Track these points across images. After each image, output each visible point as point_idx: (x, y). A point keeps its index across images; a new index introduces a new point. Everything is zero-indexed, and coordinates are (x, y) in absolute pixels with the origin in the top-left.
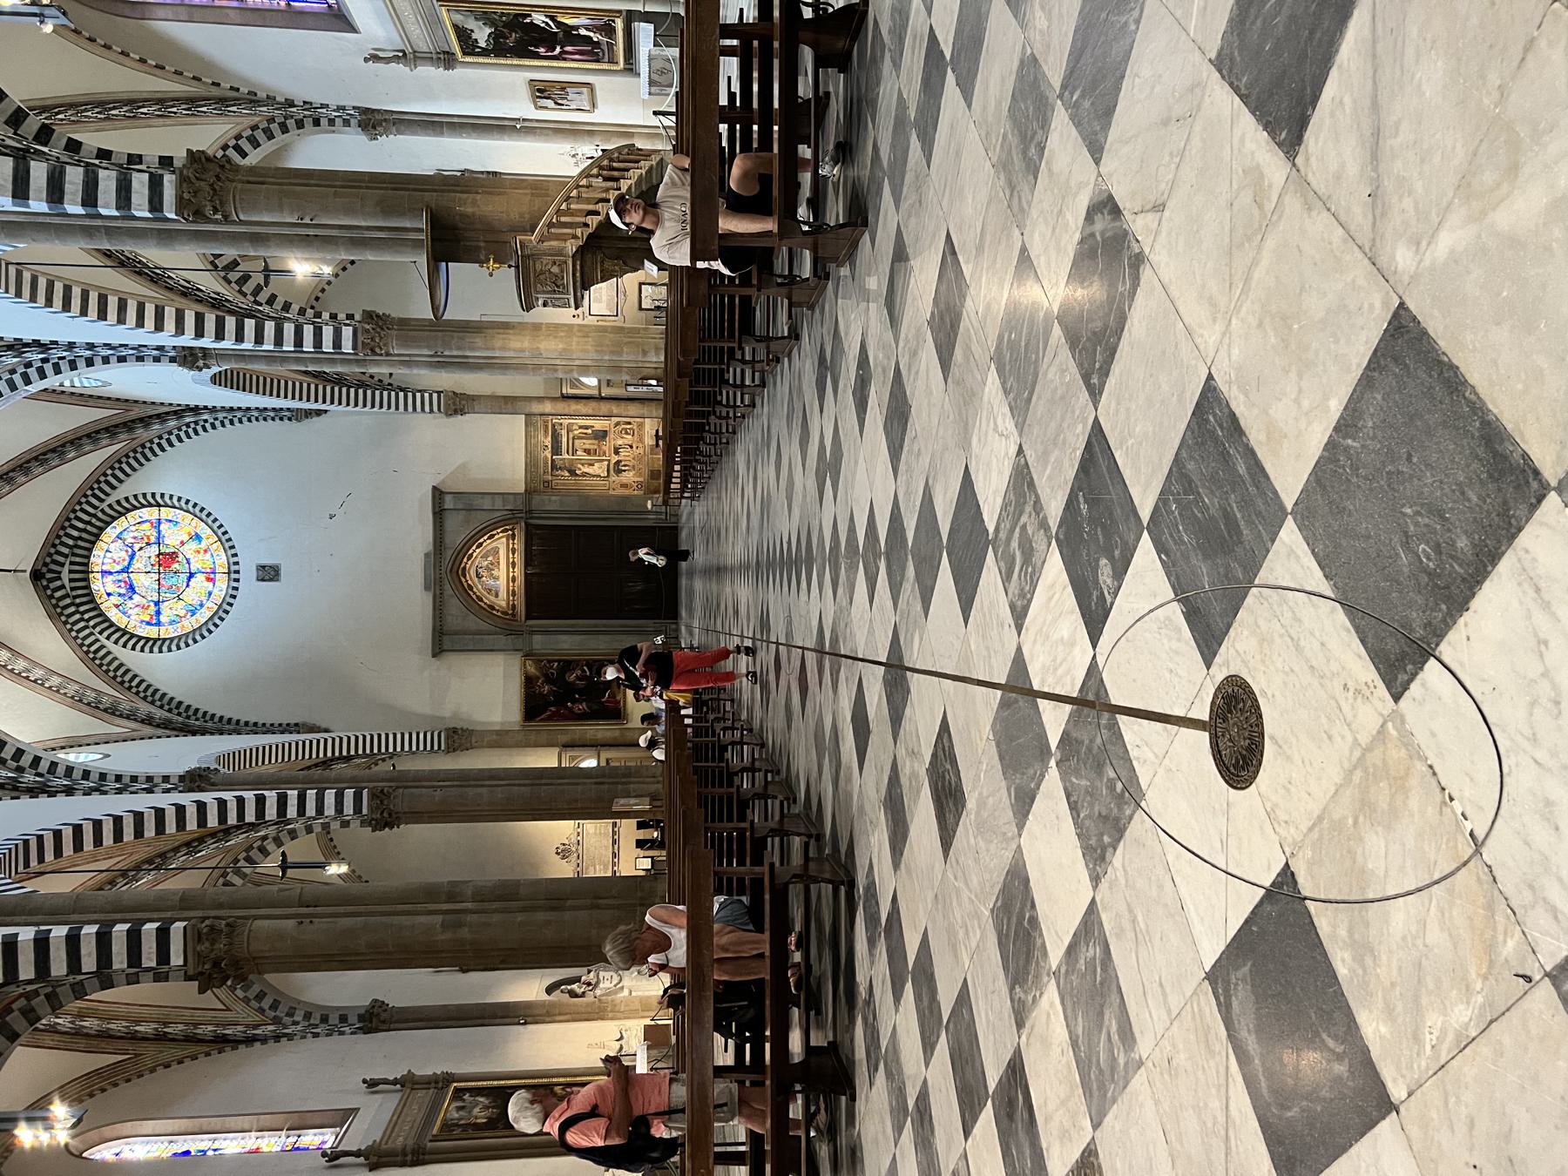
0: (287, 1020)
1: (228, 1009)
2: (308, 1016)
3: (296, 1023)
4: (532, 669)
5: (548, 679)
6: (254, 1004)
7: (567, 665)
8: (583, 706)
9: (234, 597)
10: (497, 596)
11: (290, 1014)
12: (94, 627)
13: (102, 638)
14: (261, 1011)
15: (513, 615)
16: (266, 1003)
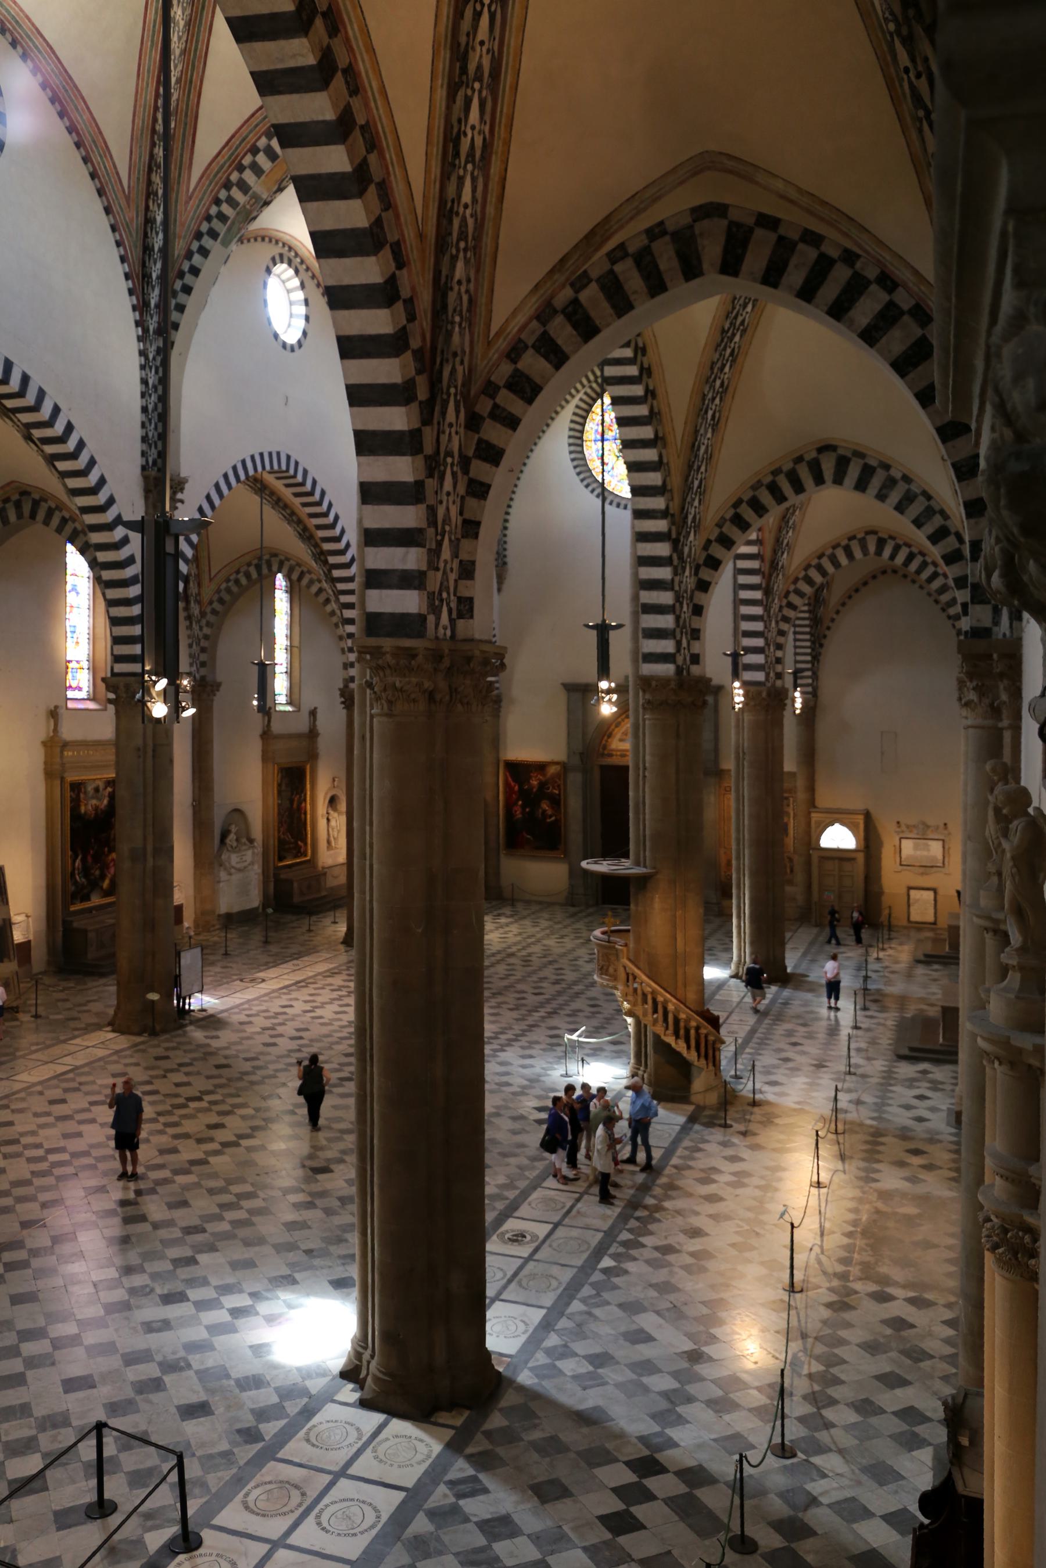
0: (204, 622)
1: (211, 580)
2: (206, 637)
3: (201, 628)
4: (552, 770)
5: (542, 785)
6: (216, 598)
7: (556, 802)
8: (519, 815)
9: (618, 505)
10: (621, 740)
11: (208, 624)
12: (591, 387)
13: (581, 395)
14: (211, 603)
15: (603, 755)
16: (216, 606)
